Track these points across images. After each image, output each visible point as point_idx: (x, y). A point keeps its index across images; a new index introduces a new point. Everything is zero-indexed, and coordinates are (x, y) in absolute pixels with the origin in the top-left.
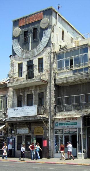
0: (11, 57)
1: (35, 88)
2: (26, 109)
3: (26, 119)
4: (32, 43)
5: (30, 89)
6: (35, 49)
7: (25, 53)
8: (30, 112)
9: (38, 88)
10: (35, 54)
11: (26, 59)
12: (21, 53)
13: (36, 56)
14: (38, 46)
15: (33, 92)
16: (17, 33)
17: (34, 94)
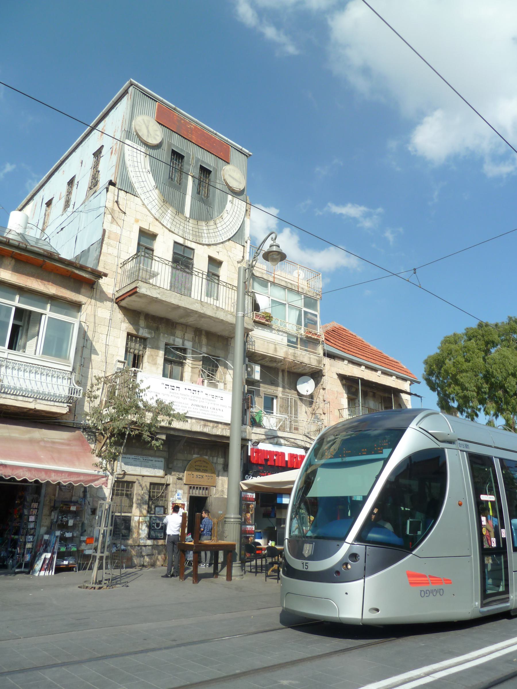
0: (111, 187)
1: (195, 335)
2: (210, 398)
3: (206, 430)
4: (192, 197)
5: (179, 333)
6: (204, 224)
7: (169, 211)
8: (221, 408)
9: (204, 341)
10: (204, 240)
11: (170, 231)
12: (156, 201)
13: (203, 245)
14: (212, 223)
15: (188, 345)
16: (148, 132)
17: (189, 351)
